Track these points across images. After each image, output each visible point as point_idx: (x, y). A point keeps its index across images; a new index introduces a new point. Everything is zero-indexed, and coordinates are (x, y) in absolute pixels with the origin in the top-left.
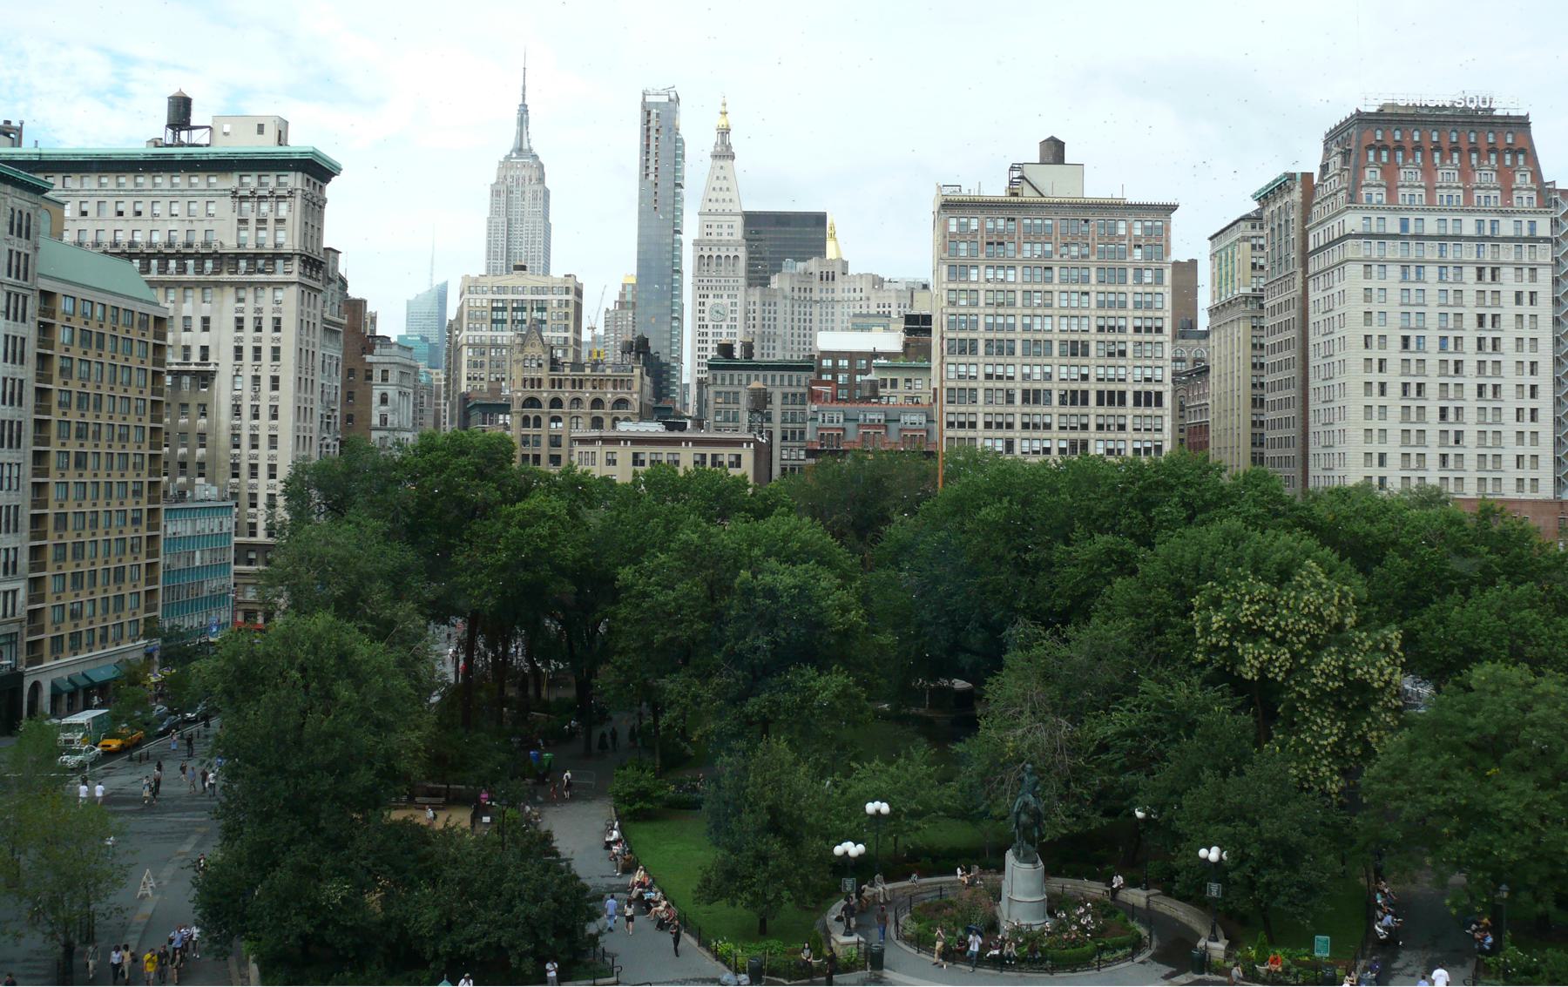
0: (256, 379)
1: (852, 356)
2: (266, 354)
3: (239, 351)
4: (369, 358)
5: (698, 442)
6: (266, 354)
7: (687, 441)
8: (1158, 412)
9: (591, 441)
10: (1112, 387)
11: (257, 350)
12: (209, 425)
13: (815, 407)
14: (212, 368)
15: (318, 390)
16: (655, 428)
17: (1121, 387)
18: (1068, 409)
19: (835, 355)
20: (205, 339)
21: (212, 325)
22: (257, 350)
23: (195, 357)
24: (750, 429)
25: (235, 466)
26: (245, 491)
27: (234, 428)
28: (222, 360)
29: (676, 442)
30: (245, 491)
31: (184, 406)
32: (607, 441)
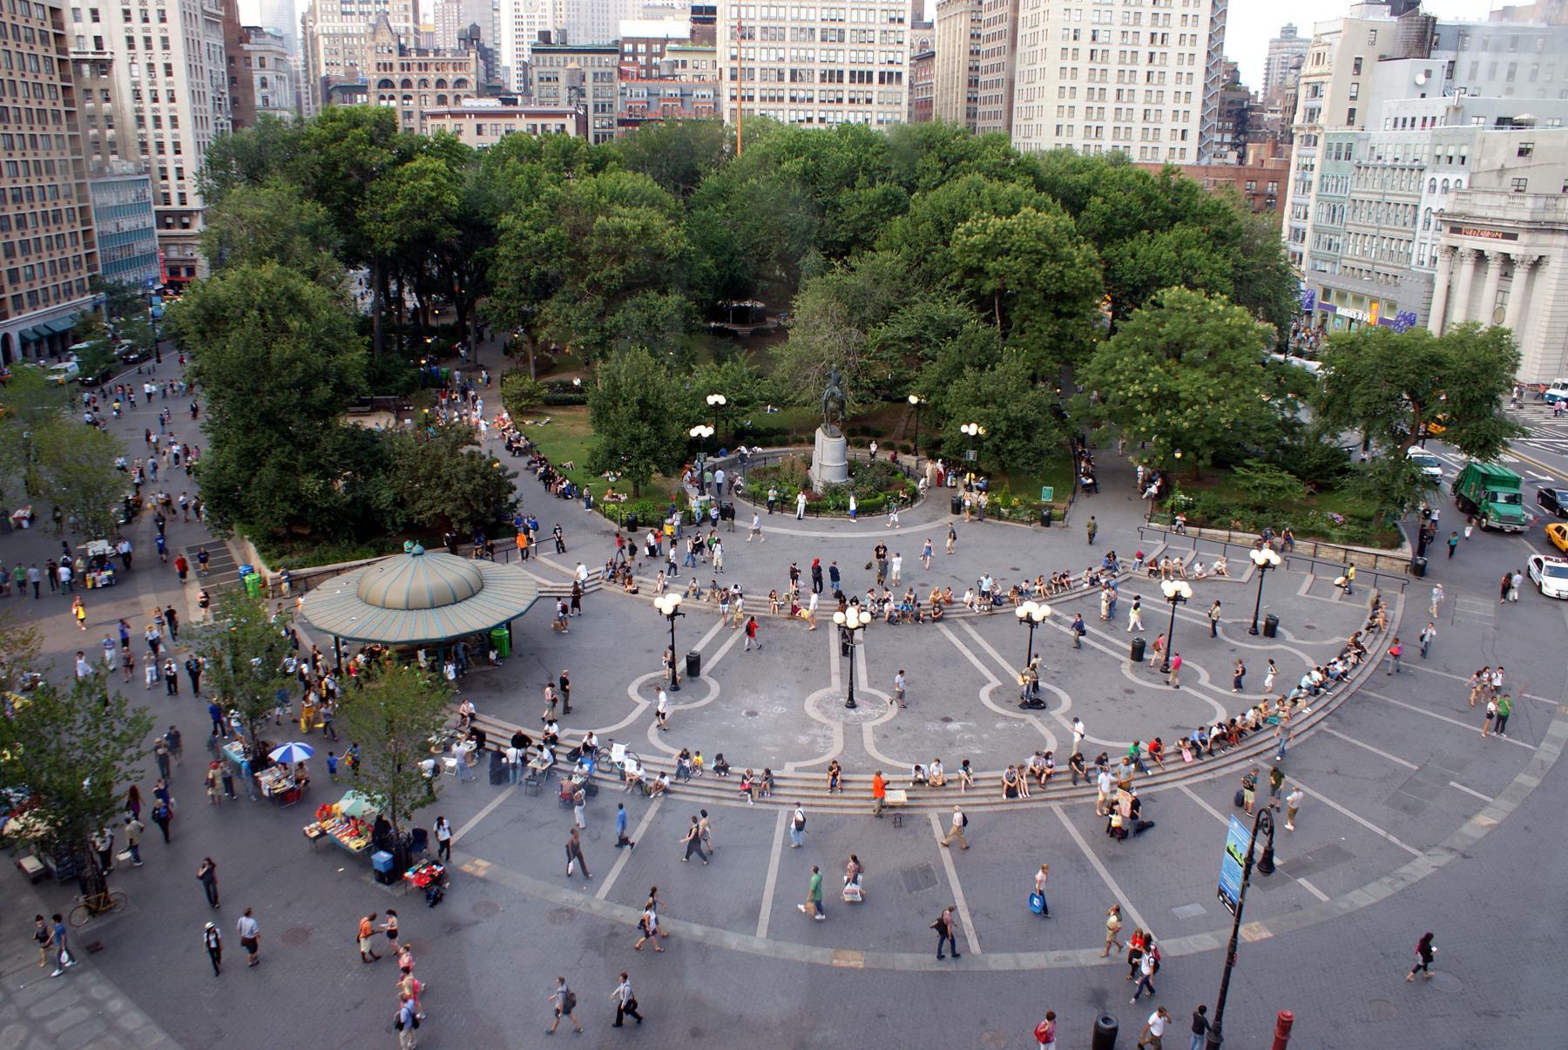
0: (151, 66)
1: (649, 42)
2: (157, 44)
3: (130, 39)
4: (246, 47)
5: (529, 115)
6: (157, 44)
7: (520, 113)
8: (898, 88)
9: (440, 115)
10: (862, 68)
11: (148, 40)
12: (115, 107)
13: (623, 84)
14: (108, 56)
15: (207, 75)
16: (493, 104)
17: (870, 68)
18: (827, 86)
19: (635, 41)
20: (96, 29)
21: (101, 16)
22: (148, 40)
23: (91, 47)
24: (570, 103)
25: (143, 144)
26: (156, 166)
27: (138, 110)
28: (115, 47)
29: (512, 115)
30: (156, 166)
31: (88, 91)
32: (454, 115)
